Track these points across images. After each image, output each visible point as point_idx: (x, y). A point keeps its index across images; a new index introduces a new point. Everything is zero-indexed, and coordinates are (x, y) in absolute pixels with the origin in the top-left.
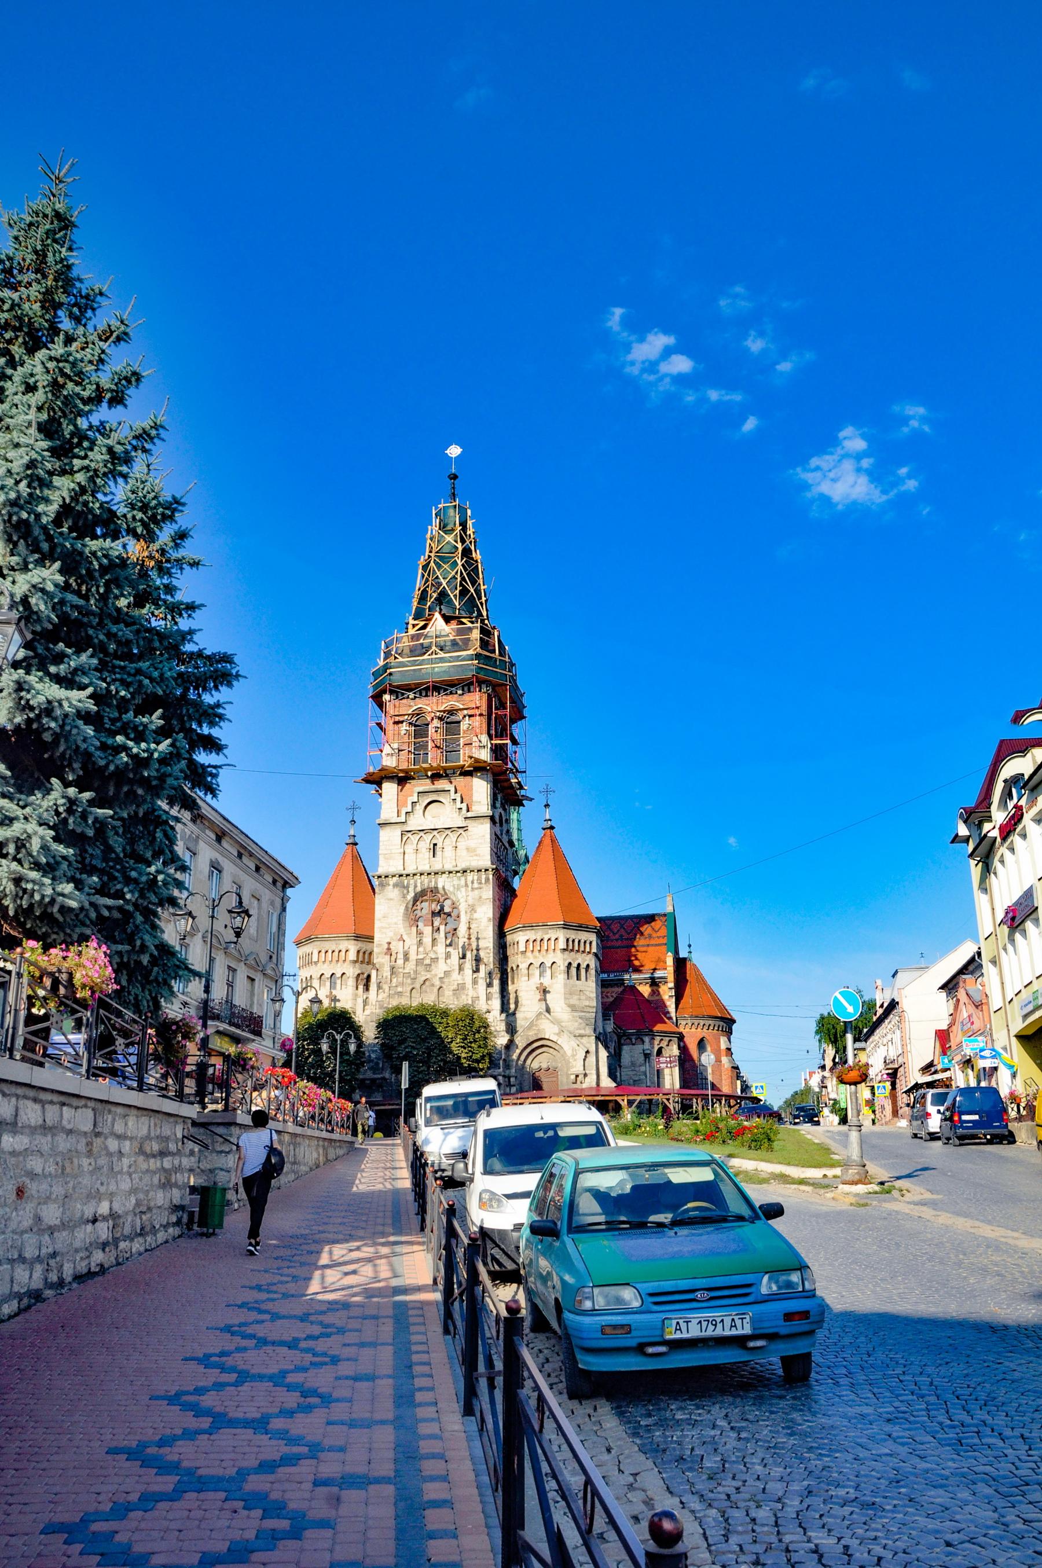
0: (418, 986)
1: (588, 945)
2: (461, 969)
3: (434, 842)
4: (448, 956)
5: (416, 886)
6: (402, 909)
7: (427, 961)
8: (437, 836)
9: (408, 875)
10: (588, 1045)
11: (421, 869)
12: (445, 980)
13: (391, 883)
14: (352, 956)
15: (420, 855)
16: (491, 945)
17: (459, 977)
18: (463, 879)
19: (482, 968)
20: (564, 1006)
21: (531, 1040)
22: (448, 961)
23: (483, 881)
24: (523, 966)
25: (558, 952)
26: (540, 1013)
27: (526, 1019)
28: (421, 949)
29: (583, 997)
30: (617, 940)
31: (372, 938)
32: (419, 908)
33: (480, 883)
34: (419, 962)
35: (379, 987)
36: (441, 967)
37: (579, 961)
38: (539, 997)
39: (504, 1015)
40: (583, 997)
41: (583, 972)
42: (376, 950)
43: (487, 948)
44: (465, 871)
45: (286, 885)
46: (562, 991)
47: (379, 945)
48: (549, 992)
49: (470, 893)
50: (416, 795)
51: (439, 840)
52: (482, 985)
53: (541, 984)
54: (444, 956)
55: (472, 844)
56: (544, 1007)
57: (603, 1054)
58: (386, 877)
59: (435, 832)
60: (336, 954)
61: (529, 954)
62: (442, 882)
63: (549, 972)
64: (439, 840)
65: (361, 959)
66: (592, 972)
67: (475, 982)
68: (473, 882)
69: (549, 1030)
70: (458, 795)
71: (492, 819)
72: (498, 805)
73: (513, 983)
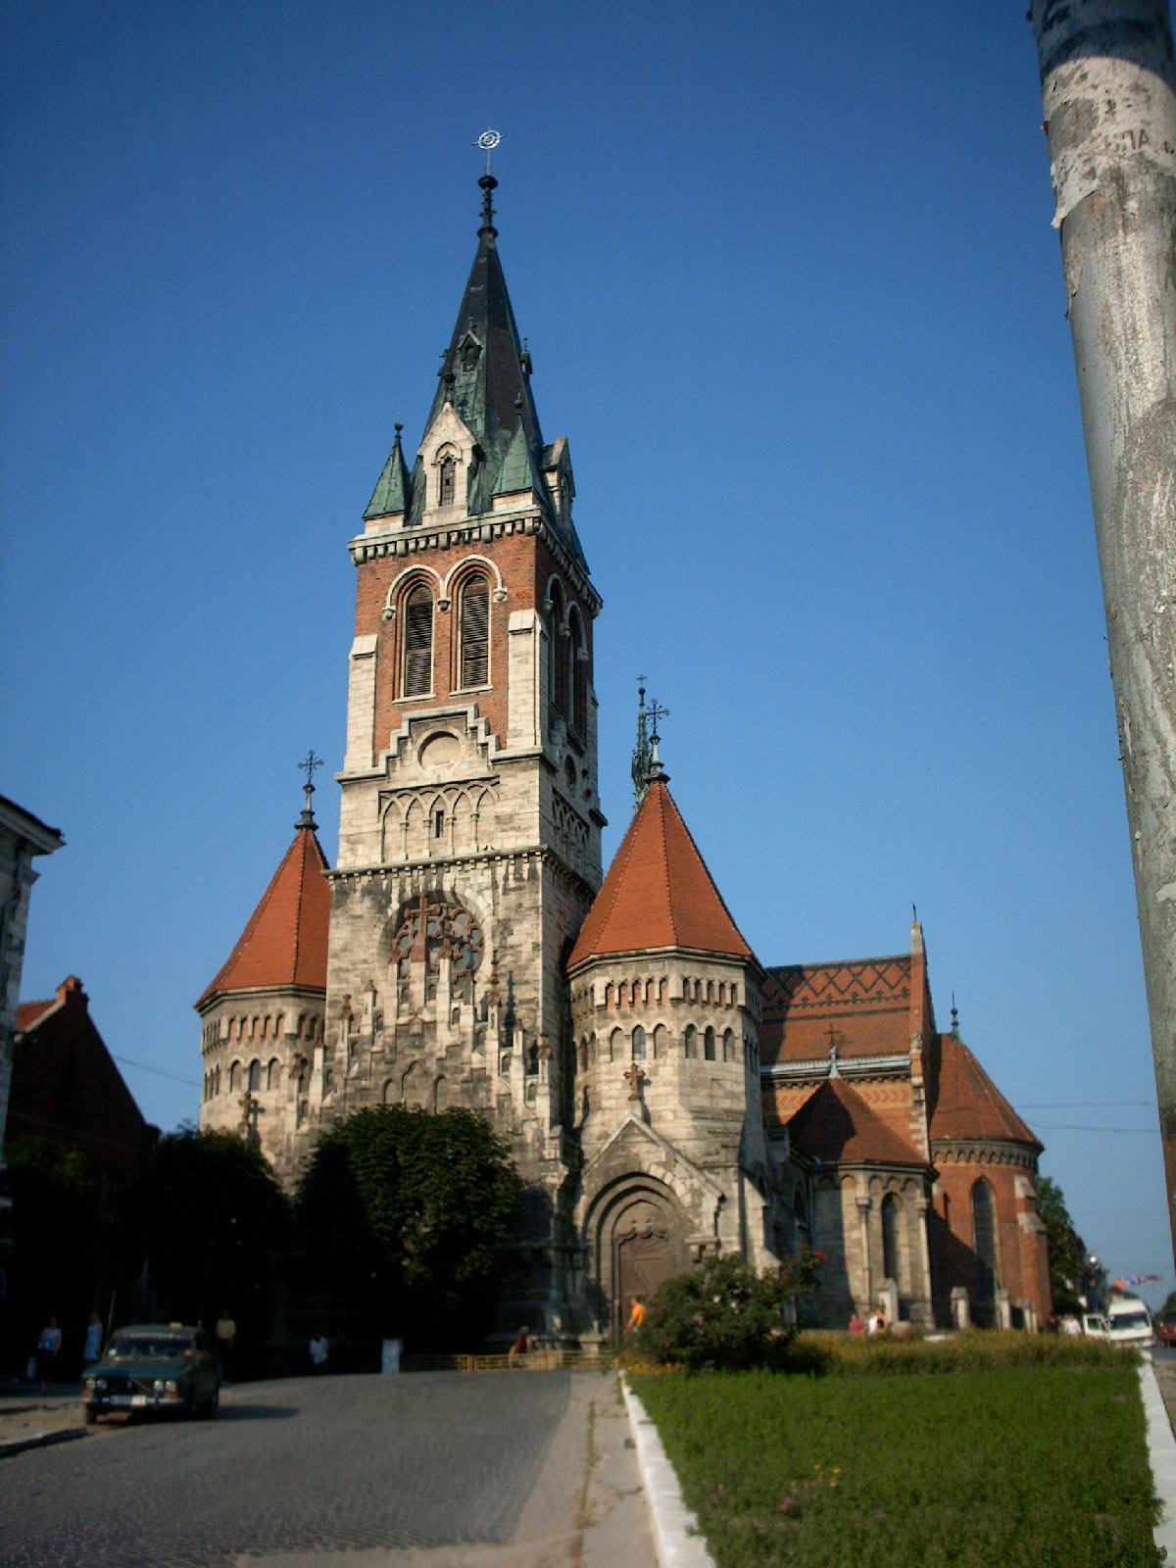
0: (398, 1075)
1: (728, 992)
2: (478, 1039)
3: (438, 807)
4: (455, 1016)
5: (402, 891)
6: (377, 934)
7: (416, 1029)
8: (444, 797)
9: (388, 871)
10: (724, 1186)
11: (414, 858)
12: (449, 1063)
13: (359, 887)
14: (289, 1025)
15: (413, 835)
16: (540, 995)
17: (476, 1057)
18: (488, 872)
19: (518, 1037)
20: (680, 1108)
21: (613, 1176)
22: (455, 1027)
23: (525, 875)
24: (602, 1034)
25: (668, 1004)
26: (631, 1124)
27: (606, 1136)
28: (405, 1006)
29: (720, 1092)
30: (821, 1004)
31: (323, 991)
32: (410, 931)
33: (519, 879)
34: (401, 1031)
35: (328, 1083)
36: (445, 1037)
37: (711, 1022)
38: (629, 1092)
39: (558, 1129)
40: (720, 1092)
41: (718, 1043)
42: (328, 1012)
43: (531, 1001)
44: (491, 859)
45: (25, 847)
46: (676, 1079)
47: (333, 1003)
48: (648, 1083)
49: (501, 897)
50: (405, 725)
51: (448, 804)
52: (517, 1069)
53: (635, 1067)
54: (447, 1019)
55: (505, 808)
56: (639, 1112)
57: (755, 1202)
58: (350, 875)
59: (440, 792)
60: (260, 1023)
61: (612, 1010)
62: (449, 880)
63: (649, 1044)
64: (448, 804)
65: (305, 1031)
66: (739, 1044)
67: (505, 1065)
68: (506, 879)
69: (650, 1159)
70: (482, 719)
71: (544, 761)
72: (560, 737)
73: (586, 1068)
